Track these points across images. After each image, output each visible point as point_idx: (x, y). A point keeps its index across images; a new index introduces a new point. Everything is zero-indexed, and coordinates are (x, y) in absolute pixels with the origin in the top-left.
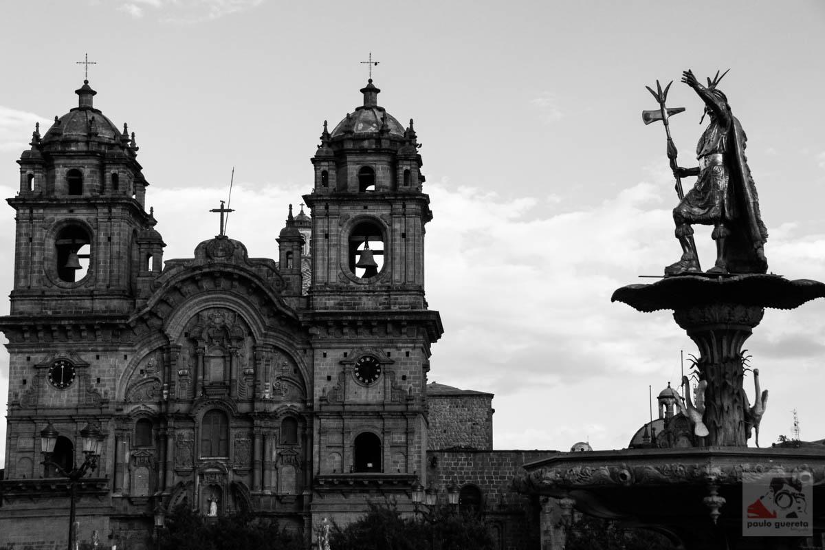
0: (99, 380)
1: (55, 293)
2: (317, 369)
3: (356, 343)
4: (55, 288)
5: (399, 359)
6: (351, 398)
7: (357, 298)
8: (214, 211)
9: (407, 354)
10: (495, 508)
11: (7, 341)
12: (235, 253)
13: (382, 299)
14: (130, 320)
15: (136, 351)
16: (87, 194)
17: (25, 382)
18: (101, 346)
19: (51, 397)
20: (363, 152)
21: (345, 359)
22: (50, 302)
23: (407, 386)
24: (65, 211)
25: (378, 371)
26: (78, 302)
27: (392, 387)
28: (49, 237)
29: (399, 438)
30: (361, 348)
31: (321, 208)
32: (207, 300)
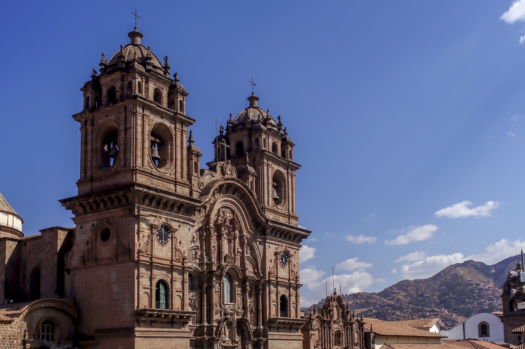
0: (180, 242)
1: (156, 174)
7: (278, 216)
9: (295, 252)
19: (158, 250)
21: (276, 251)
22: (154, 180)
26: (168, 184)
27: (292, 270)
30: (282, 246)
32: (225, 201)
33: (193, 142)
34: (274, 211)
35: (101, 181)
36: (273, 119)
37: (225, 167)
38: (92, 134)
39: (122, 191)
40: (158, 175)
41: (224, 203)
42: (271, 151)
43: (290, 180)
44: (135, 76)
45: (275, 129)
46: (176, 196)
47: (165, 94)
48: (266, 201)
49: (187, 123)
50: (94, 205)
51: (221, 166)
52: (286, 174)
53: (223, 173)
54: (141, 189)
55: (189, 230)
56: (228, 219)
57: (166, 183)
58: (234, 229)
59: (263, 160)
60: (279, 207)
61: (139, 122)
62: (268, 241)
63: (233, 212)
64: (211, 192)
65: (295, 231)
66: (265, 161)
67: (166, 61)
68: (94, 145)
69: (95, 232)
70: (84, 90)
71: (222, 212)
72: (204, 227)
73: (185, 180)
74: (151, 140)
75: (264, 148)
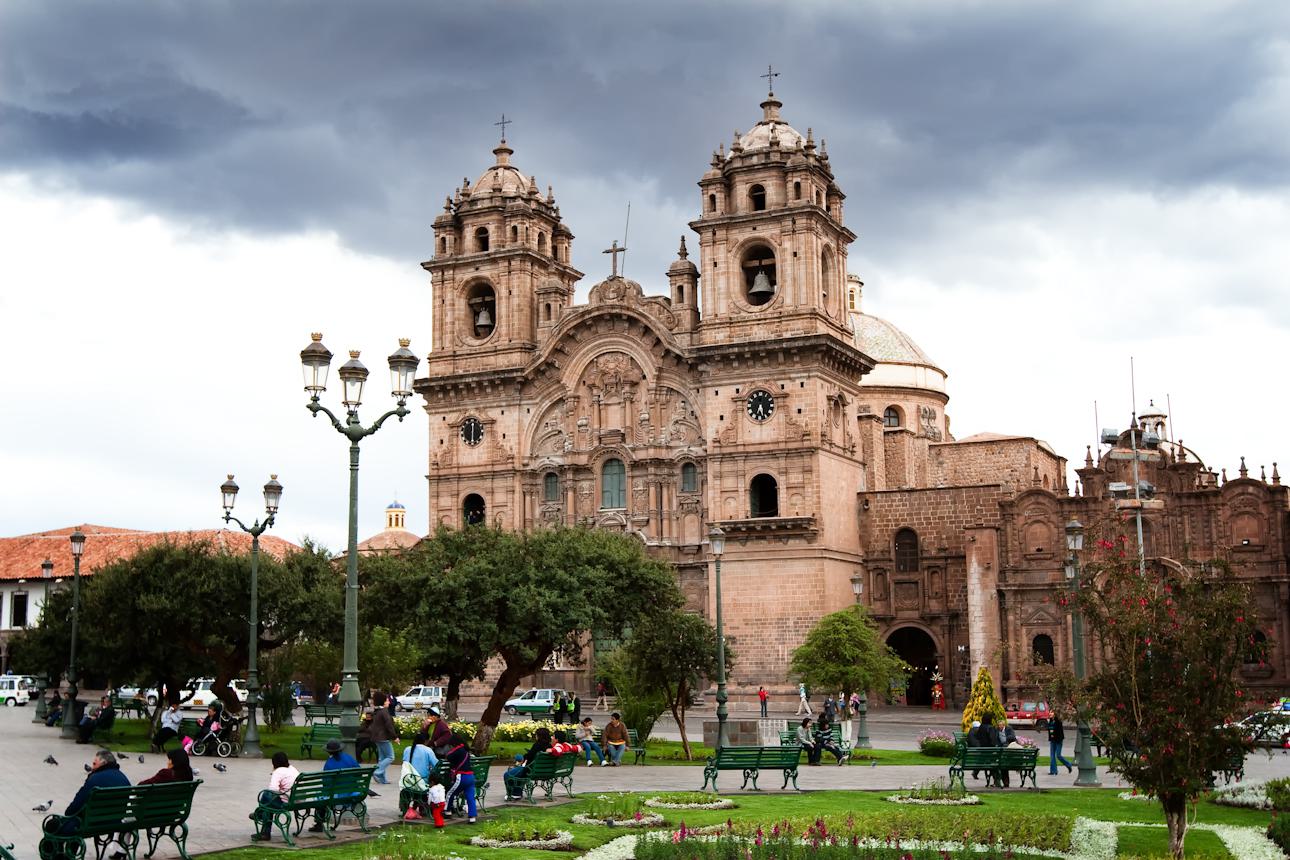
1: (465, 352)
2: (709, 409)
3: (748, 377)
4: (465, 347)
5: (792, 391)
6: (748, 439)
8: (607, 252)
10: (933, 552)
11: (425, 403)
12: (627, 294)
13: (773, 327)
14: (526, 372)
16: (492, 250)
17: (442, 442)
18: (506, 401)
20: (751, 169)
23: (802, 420)
24: (472, 269)
25: (772, 405)
28: (460, 297)
29: (795, 478)
31: (708, 235)
32: (599, 346)
40: (468, 352)
62: (709, 383)
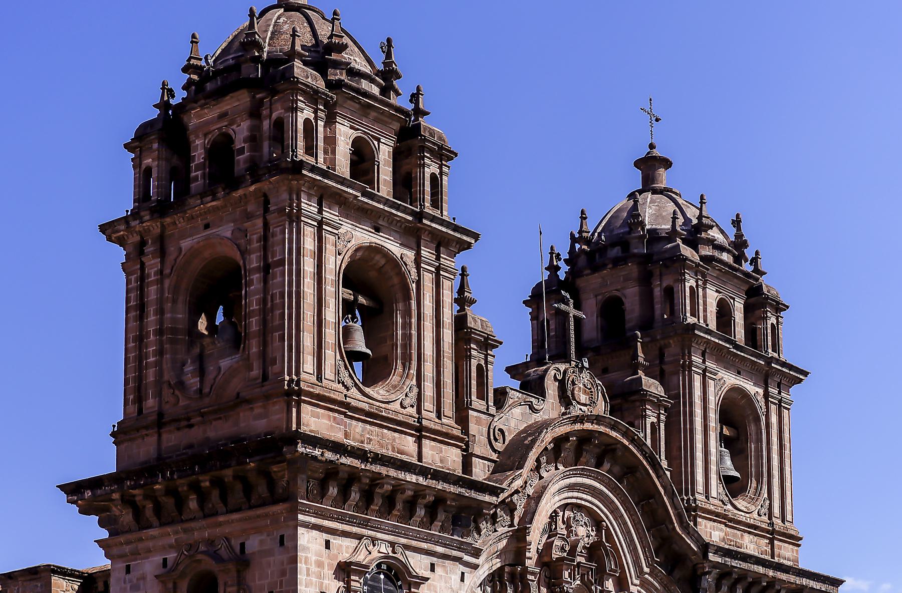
7: (739, 533)
15: (475, 567)
22: (354, 422)
26: (396, 435)
32: (571, 487)
33: (472, 302)
34: (725, 517)
35: (191, 426)
36: (717, 226)
37: (571, 379)
38: (160, 282)
39: (258, 458)
40: (366, 407)
41: (571, 494)
42: (713, 326)
43: (774, 419)
44: (423, 158)
45: (725, 257)
46: (424, 472)
47: (384, 154)
48: (700, 488)
49: (455, 243)
50: (169, 502)
51: (559, 378)
52: (761, 398)
53: (566, 399)
54: (317, 452)
55: (462, 580)
56: (581, 545)
57: (390, 432)
58: (601, 574)
59: (690, 358)
60: (740, 503)
61: (309, 243)
63: (597, 523)
64: (530, 462)
65: (792, 578)
66: (697, 359)
67: (389, 55)
68: (168, 315)
69: (170, 585)
70: (136, 147)
71: (564, 522)
72: (507, 569)
73: (449, 422)
74: (343, 299)
75: (691, 320)
